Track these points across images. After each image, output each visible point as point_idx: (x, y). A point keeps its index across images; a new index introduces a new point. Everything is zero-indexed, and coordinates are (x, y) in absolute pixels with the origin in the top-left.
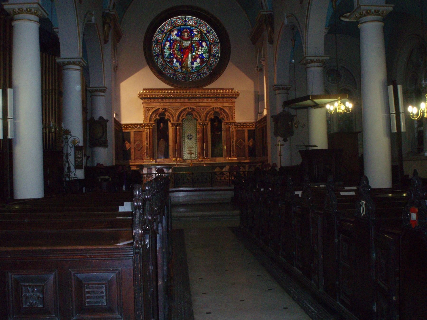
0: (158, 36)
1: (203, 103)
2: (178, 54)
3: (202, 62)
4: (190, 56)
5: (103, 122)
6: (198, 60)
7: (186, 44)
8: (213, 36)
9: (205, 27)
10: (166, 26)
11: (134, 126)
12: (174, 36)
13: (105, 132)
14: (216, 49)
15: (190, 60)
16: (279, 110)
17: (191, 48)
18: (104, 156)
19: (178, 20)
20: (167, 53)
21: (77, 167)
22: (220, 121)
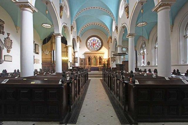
0: (89, 41)
1: (97, 55)
2: (93, 45)
3: (98, 46)
4: (95, 45)
5: (77, 58)
6: (97, 46)
7: (94, 43)
8: (100, 41)
9: (98, 39)
10: (90, 39)
11: (83, 59)
12: (92, 41)
13: (77, 60)
14: (100, 44)
15: (95, 46)
16: (113, 56)
17: (95, 44)
18: (77, 65)
19: (93, 38)
20: (90, 45)
21: (71, 67)
22: (101, 58)
